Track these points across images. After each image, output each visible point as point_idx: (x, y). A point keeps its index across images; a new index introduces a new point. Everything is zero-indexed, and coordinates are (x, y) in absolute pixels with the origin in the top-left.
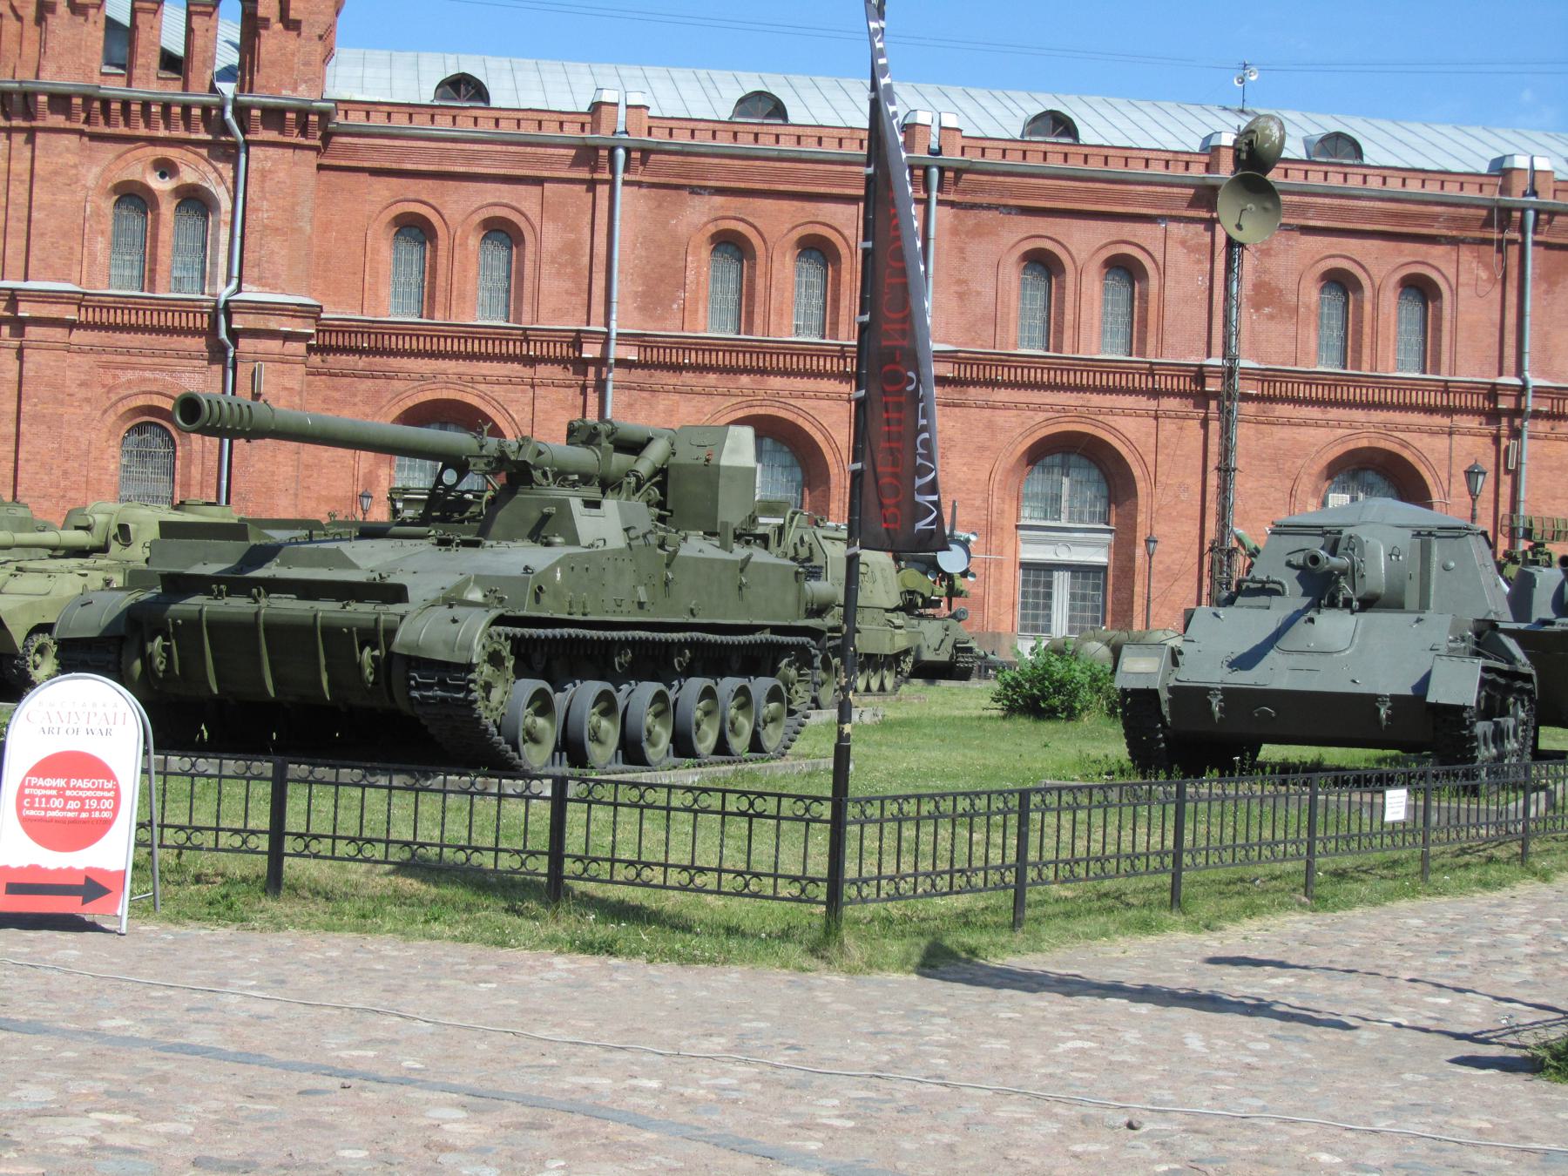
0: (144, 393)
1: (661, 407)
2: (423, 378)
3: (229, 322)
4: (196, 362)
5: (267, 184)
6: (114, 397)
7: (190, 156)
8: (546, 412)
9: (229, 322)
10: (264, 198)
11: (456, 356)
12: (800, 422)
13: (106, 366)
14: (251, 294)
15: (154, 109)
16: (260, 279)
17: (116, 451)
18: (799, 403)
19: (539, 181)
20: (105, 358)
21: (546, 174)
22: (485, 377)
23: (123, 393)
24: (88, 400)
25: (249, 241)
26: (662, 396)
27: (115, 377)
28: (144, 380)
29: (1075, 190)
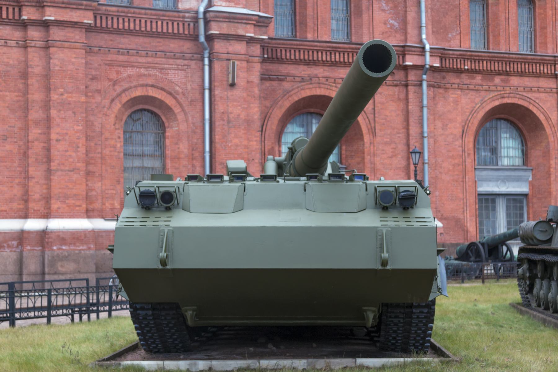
0: (142, 85)
1: (451, 99)
2: (303, 80)
3: (207, 28)
4: (179, 62)
6: (118, 89)
8: (383, 104)
11: (324, 63)
12: (531, 107)
13: (110, 65)
17: (120, 133)
18: (529, 95)
20: (110, 57)
23: (125, 85)
24: (99, 91)
26: (451, 91)
27: (118, 73)
28: (141, 76)
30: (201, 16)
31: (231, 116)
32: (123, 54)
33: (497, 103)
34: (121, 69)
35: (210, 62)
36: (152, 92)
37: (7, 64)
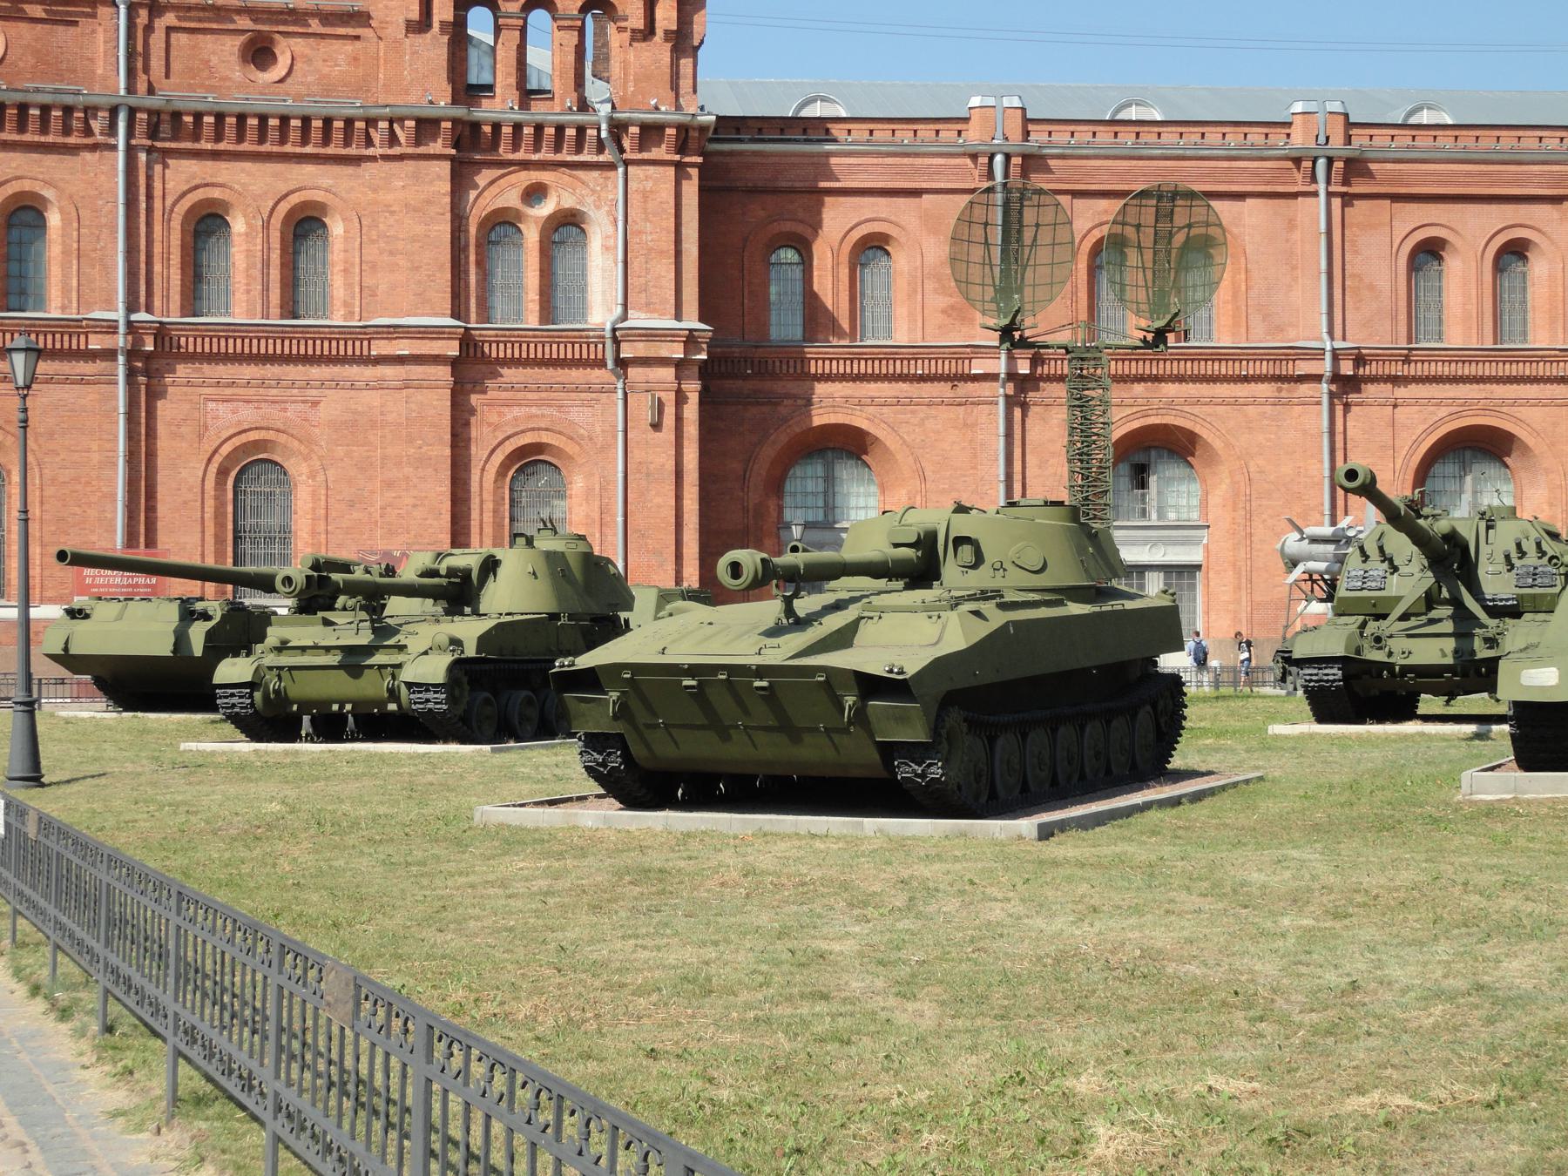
0: (533, 429)
4: (583, 395)
5: (650, 205)
7: (566, 178)
9: (618, 351)
10: (647, 220)
11: (843, 378)
12: (1197, 430)
14: (638, 320)
15: (526, 131)
16: (647, 304)
19: (916, 193)
21: (925, 185)
22: (872, 399)
25: (634, 265)
27: (500, 414)
28: (531, 417)
29: (1468, 174)
30: (608, 334)
31: (652, 467)
32: (506, 390)
33: (1136, 425)
34: (505, 409)
35: (626, 394)
36: (545, 438)
37: (355, 412)
